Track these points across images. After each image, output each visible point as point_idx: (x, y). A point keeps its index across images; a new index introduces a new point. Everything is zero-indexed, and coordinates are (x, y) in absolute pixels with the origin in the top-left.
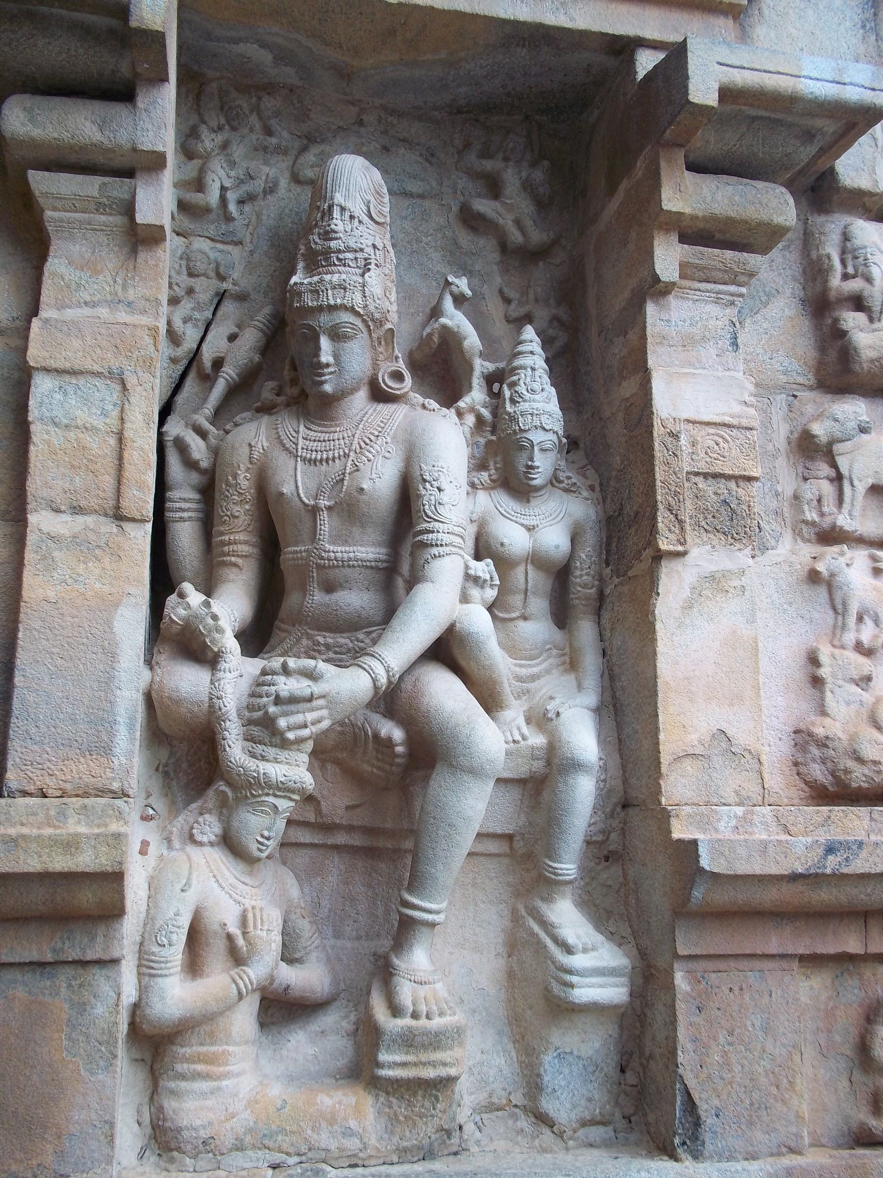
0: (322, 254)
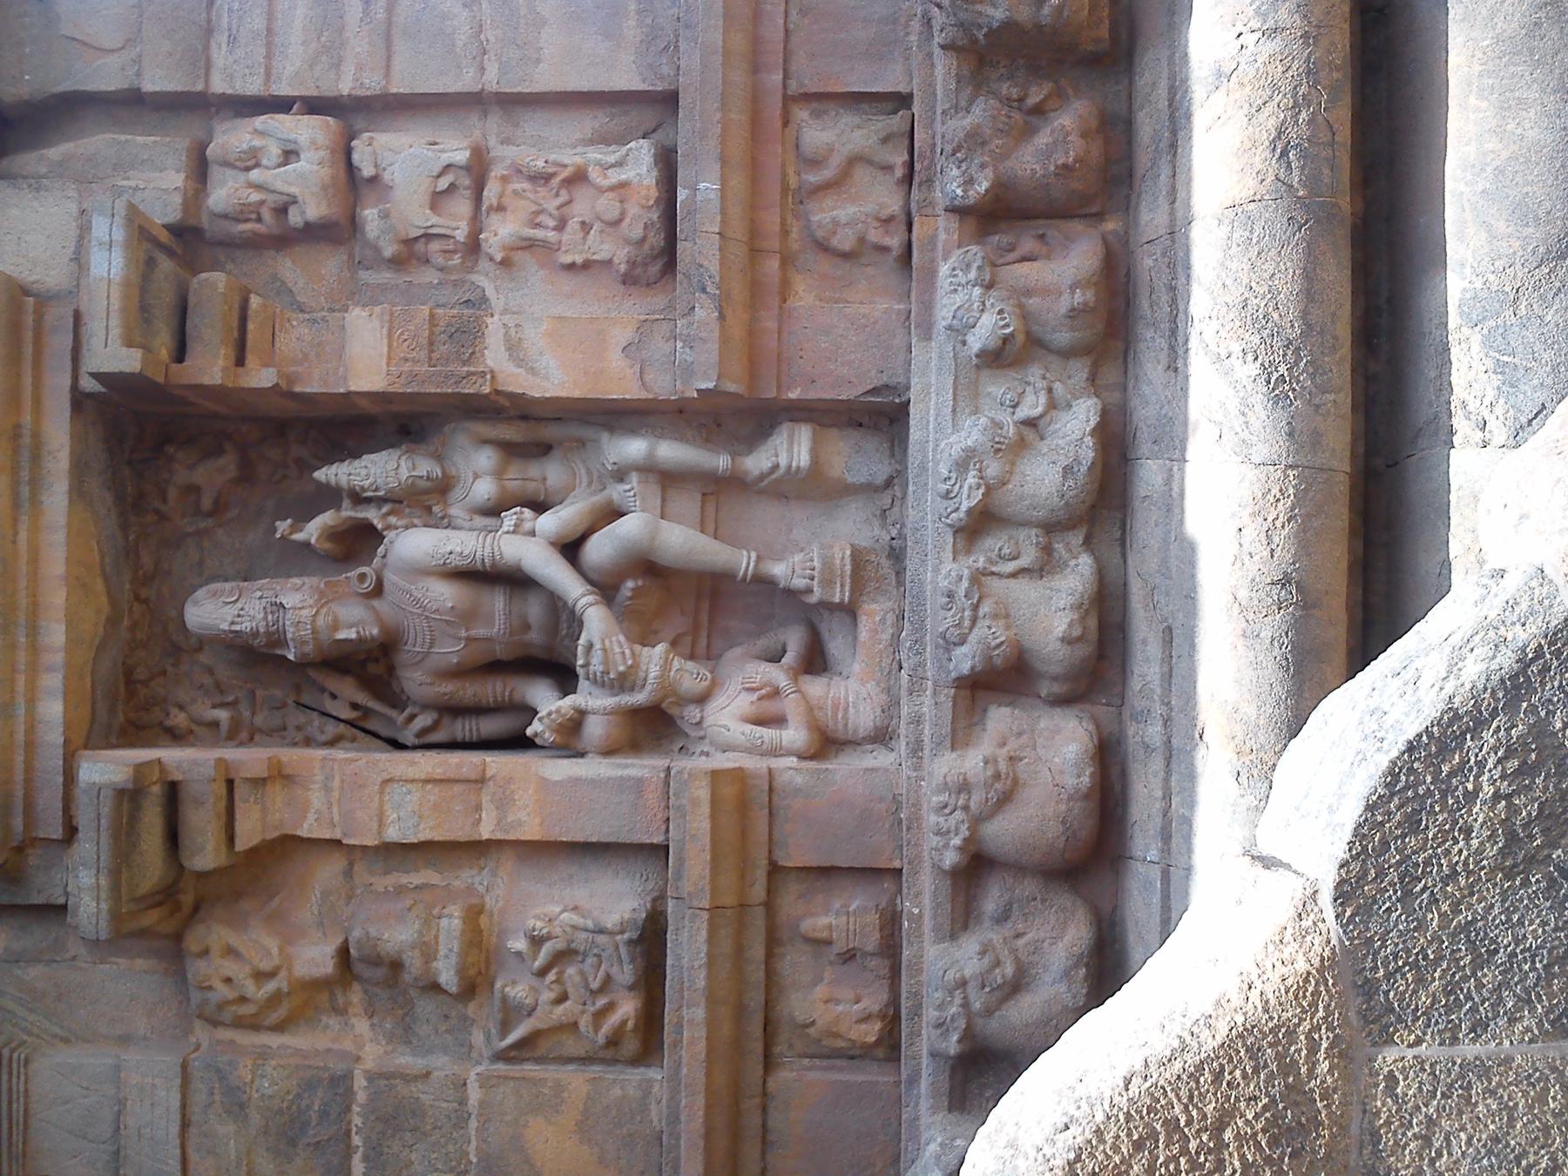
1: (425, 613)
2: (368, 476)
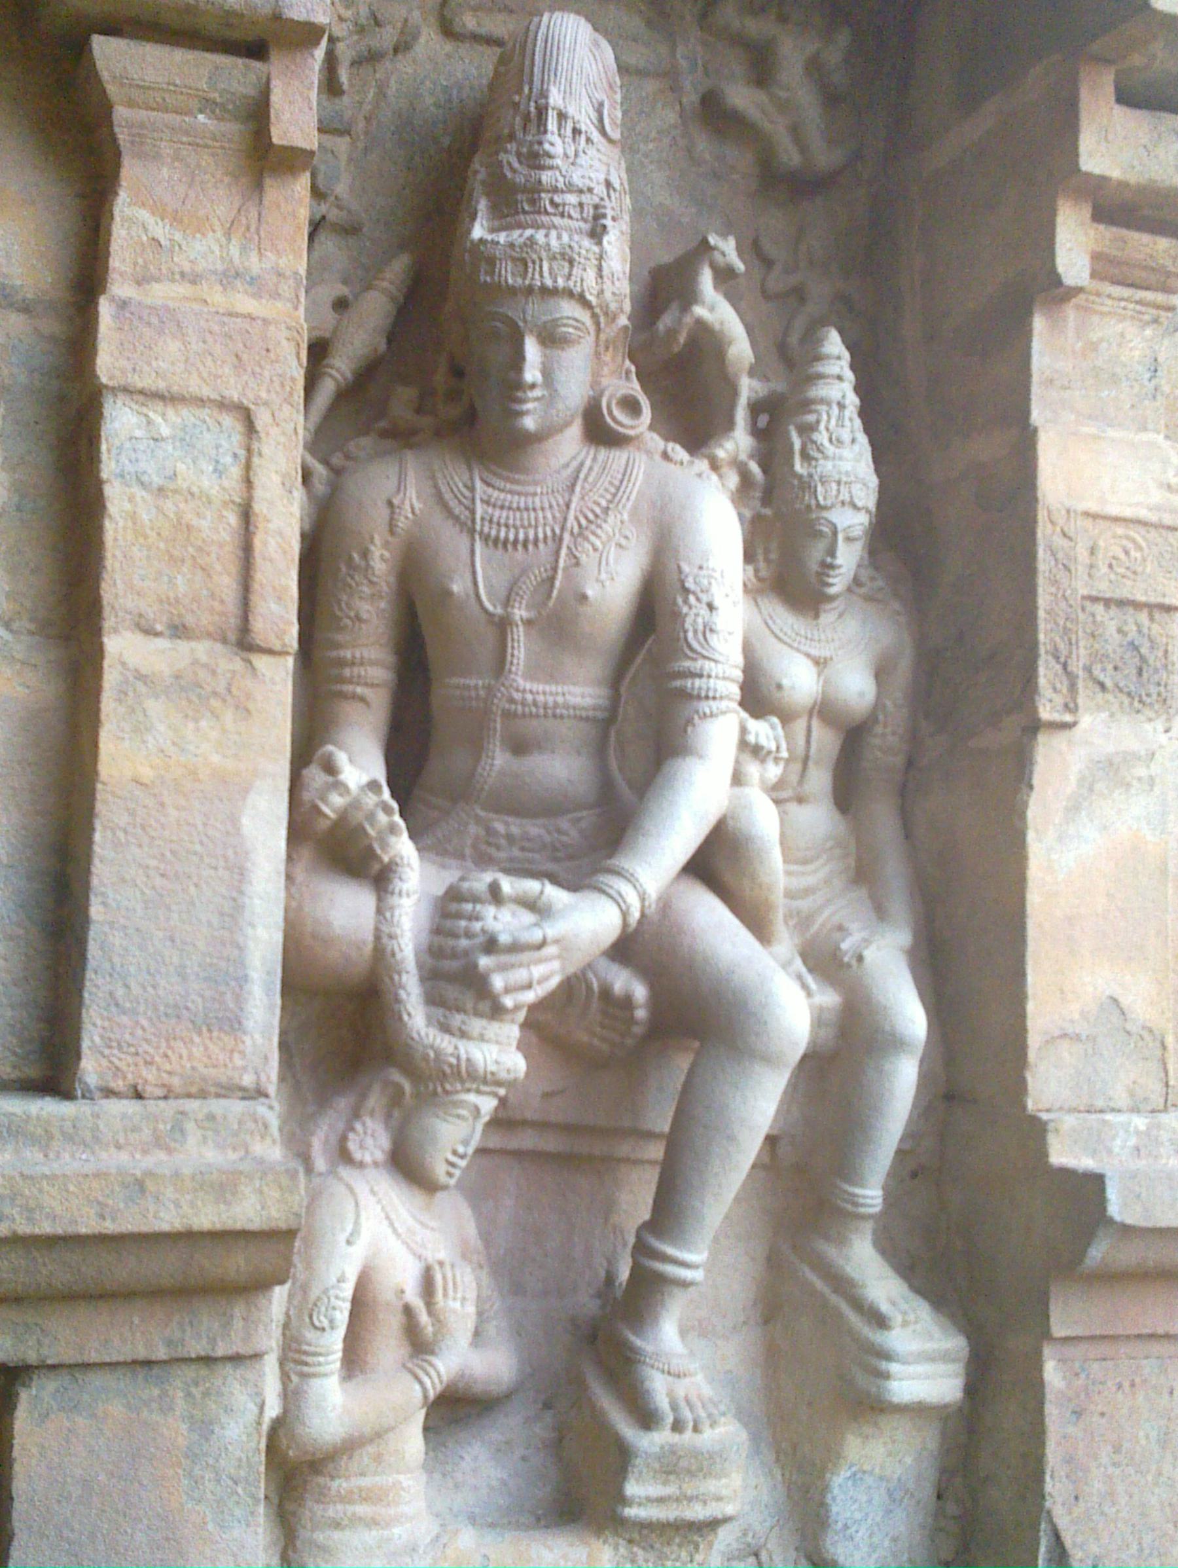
0: (525, 190)
1: (567, 537)
2: (838, 442)
